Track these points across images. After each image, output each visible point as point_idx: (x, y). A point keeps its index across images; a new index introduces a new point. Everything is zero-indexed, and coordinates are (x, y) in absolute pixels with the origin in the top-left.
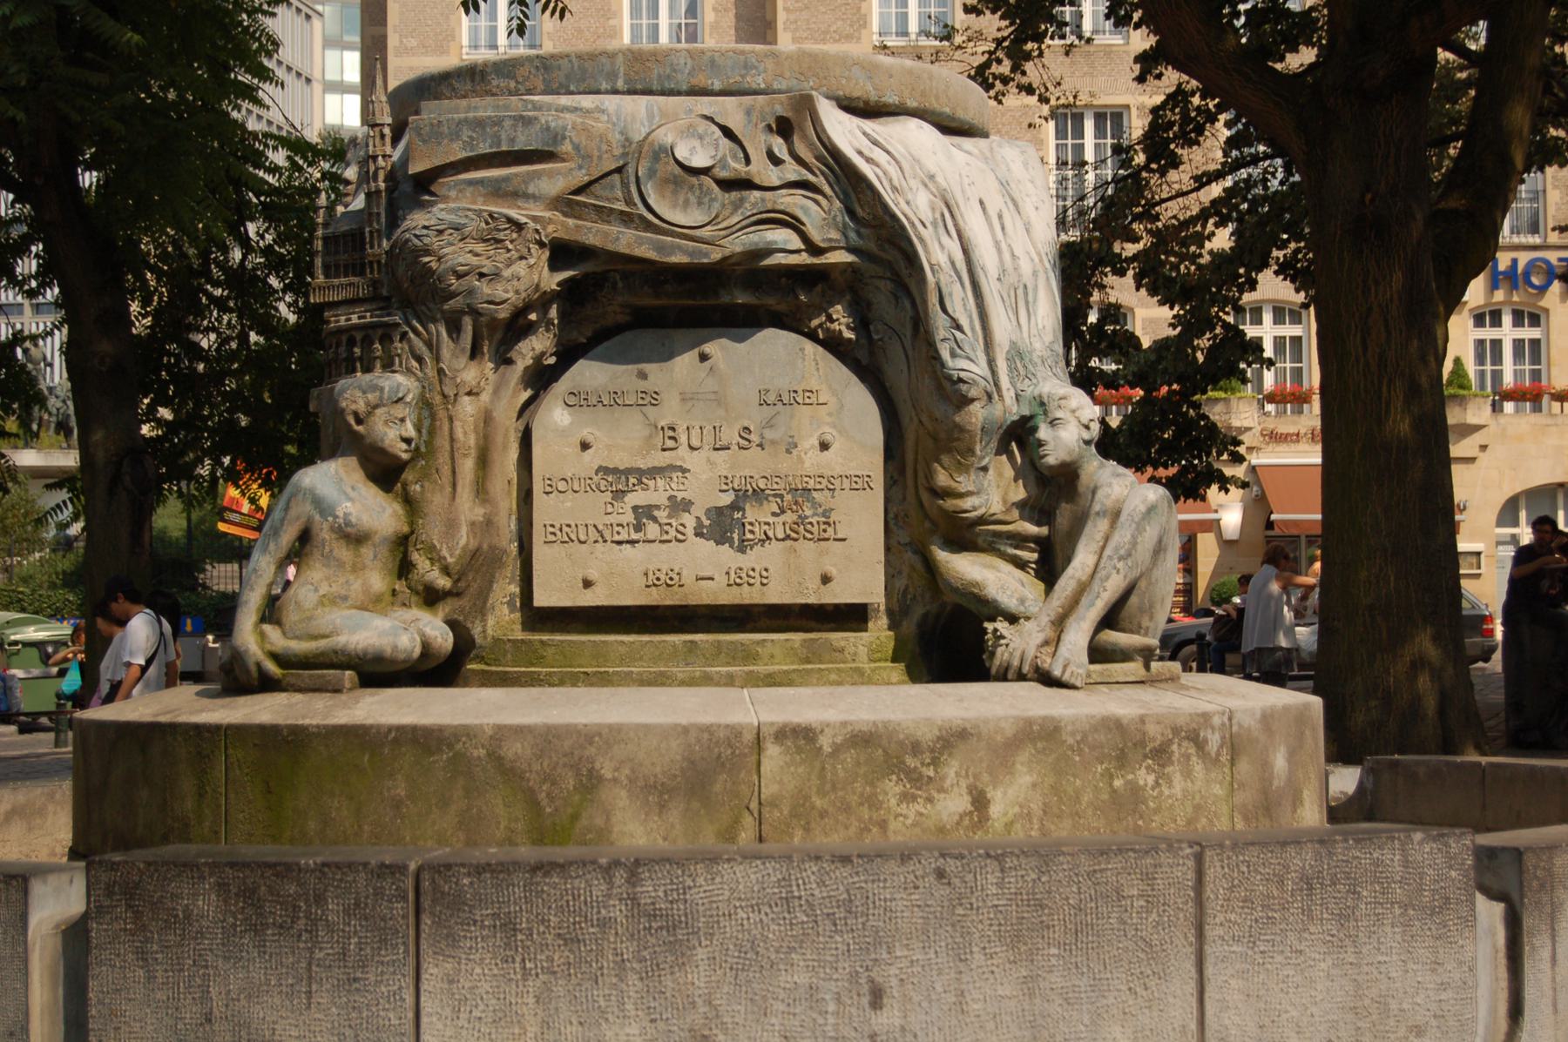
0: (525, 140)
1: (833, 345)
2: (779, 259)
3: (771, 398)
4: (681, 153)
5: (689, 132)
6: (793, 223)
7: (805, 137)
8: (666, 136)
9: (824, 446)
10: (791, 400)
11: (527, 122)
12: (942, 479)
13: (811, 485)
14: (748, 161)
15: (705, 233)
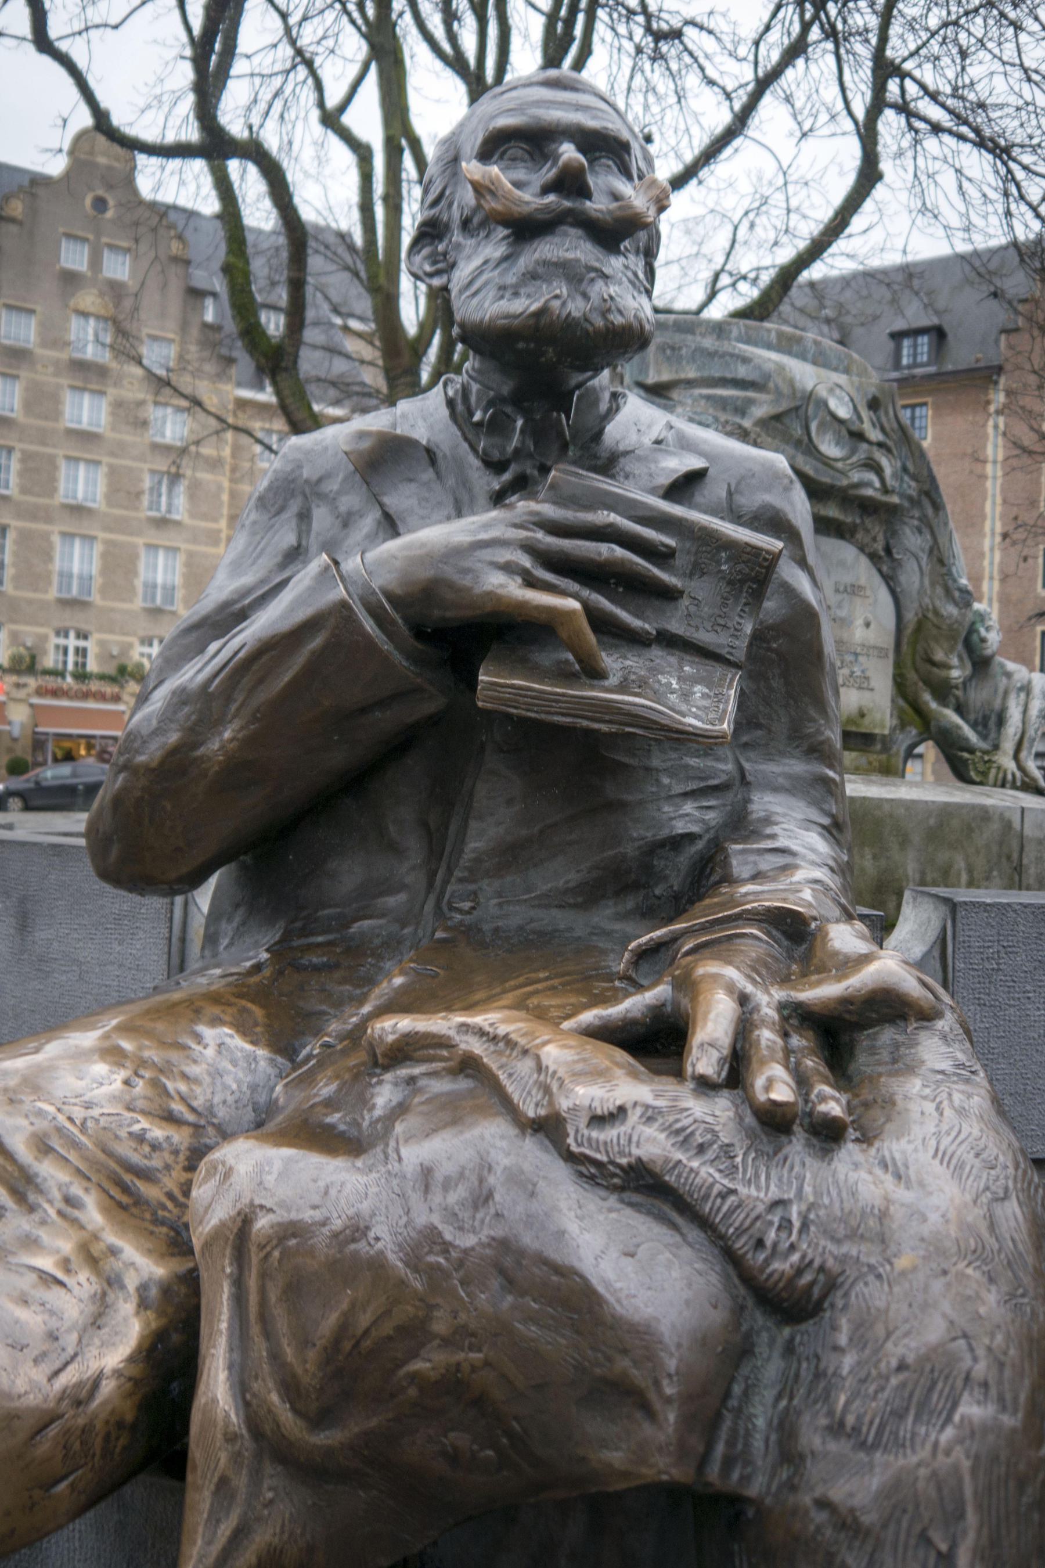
0: (742, 372)
1: (873, 557)
2: (869, 492)
3: (842, 589)
4: (833, 404)
5: (831, 391)
6: (878, 470)
7: (887, 413)
8: (822, 392)
9: (868, 625)
10: (854, 590)
11: (745, 360)
12: (939, 656)
13: (859, 650)
14: (862, 422)
15: (839, 465)
